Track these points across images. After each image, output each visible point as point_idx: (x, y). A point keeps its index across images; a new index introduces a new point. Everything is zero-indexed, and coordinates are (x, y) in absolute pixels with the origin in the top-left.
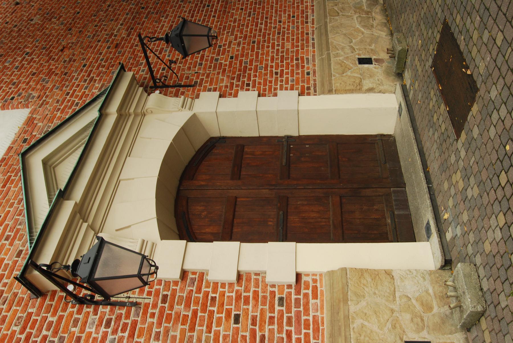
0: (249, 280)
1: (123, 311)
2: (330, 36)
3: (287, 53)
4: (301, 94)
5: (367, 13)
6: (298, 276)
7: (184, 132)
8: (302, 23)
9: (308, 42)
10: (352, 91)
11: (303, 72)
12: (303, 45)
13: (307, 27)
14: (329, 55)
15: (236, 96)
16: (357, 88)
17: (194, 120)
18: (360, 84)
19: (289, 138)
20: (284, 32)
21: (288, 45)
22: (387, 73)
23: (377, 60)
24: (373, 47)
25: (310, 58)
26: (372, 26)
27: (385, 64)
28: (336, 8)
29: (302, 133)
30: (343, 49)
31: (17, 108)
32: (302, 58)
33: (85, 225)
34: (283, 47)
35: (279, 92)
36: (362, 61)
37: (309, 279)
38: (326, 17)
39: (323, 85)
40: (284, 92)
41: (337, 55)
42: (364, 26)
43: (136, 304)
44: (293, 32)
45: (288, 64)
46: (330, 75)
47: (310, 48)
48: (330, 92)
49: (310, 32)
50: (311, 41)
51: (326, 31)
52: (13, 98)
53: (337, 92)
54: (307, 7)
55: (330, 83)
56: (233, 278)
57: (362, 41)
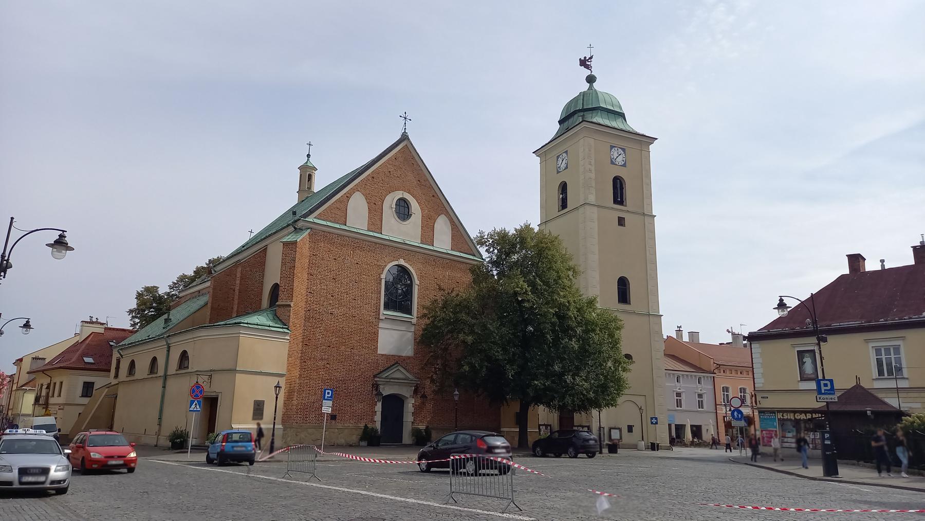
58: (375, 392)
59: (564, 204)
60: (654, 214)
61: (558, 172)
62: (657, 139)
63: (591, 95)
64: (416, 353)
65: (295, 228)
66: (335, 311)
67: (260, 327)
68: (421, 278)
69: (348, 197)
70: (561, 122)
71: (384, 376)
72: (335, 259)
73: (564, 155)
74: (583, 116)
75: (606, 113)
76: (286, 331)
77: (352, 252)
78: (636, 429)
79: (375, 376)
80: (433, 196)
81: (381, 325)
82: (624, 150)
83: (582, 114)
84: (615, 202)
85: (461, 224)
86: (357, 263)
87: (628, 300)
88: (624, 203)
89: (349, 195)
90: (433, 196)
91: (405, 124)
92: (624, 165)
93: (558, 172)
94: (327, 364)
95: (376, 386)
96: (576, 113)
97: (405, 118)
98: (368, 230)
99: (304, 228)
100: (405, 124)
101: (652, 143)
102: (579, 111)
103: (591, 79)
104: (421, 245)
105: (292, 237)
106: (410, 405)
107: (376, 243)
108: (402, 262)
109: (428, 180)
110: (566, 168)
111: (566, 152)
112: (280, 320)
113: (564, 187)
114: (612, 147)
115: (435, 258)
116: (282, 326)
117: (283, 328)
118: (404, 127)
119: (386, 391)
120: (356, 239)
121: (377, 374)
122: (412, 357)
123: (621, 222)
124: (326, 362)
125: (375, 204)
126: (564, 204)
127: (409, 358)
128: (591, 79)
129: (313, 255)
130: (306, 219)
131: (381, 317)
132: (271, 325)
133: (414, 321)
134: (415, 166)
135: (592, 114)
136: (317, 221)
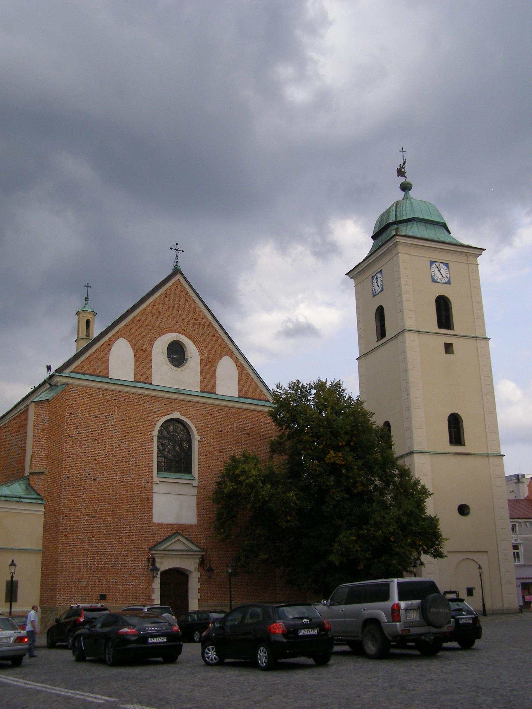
1: (147, 567)
6: (154, 600)
7: (188, 570)
15: (199, 582)
17: (191, 572)
21: (219, 595)
33: (163, 556)
40: (200, 594)
43: (148, 569)
52: (200, 516)
56: (153, 587)
58: (150, 567)
59: (382, 333)
60: (488, 336)
61: (374, 296)
62: (484, 250)
63: (405, 204)
64: (198, 522)
65: (51, 385)
66: (99, 476)
67: (8, 499)
68: (201, 432)
69: (110, 344)
70: (374, 237)
71: (162, 548)
72: (97, 417)
73: (379, 275)
74: (397, 230)
75: (423, 224)
76: (39, 501)
77: (116, 408)
78: (477, 592)
79: (150, 549)
80: (214, 336)
81: (156, 488)
82: (447, 265)
83: (395, 227)
84: (440, 326)
85: (250, 365)
86: (123, 420)
87: (463, 443)
88: (452, 326)
89: (111, 343)
90: (214, 336)
91: (177, 256)
92: (449, 283)
93: (374, 296)
94: (93, 537)
95: (152, 561)
97: (177, 250)
98: (136, 381)
99: (59, 384)
100: (177, 256)
101: (481, 255)
102: (393, 223)
103: (405, 187)
104: (201, 394)
105: (46, 395)
106: (196, 580)
107: (145, 396)
108: (176, 415)
109: (205, 318)
110: (382, 290)
111: (381, 272)
112: (34, 490)
113: (380, 312)
114: (432, 262)
115: (219, 408)
116: (34, 497)
117: (36, 499)
118: (176, 260)
119: (164, 565)
120: (121, 392)
121: (153, 547)
122: (195, 525)
123: (448, 348)
125: (142, 350)
126: (382, 333)
127: (191, 526)
128: (405, 187)
129: (71, 414)
130: (62, 375)
131: (156, 479)
132: (22, 496)
133: (196, 483)
134: (190, 303)
135: (407, 226)
136: (72, 375)
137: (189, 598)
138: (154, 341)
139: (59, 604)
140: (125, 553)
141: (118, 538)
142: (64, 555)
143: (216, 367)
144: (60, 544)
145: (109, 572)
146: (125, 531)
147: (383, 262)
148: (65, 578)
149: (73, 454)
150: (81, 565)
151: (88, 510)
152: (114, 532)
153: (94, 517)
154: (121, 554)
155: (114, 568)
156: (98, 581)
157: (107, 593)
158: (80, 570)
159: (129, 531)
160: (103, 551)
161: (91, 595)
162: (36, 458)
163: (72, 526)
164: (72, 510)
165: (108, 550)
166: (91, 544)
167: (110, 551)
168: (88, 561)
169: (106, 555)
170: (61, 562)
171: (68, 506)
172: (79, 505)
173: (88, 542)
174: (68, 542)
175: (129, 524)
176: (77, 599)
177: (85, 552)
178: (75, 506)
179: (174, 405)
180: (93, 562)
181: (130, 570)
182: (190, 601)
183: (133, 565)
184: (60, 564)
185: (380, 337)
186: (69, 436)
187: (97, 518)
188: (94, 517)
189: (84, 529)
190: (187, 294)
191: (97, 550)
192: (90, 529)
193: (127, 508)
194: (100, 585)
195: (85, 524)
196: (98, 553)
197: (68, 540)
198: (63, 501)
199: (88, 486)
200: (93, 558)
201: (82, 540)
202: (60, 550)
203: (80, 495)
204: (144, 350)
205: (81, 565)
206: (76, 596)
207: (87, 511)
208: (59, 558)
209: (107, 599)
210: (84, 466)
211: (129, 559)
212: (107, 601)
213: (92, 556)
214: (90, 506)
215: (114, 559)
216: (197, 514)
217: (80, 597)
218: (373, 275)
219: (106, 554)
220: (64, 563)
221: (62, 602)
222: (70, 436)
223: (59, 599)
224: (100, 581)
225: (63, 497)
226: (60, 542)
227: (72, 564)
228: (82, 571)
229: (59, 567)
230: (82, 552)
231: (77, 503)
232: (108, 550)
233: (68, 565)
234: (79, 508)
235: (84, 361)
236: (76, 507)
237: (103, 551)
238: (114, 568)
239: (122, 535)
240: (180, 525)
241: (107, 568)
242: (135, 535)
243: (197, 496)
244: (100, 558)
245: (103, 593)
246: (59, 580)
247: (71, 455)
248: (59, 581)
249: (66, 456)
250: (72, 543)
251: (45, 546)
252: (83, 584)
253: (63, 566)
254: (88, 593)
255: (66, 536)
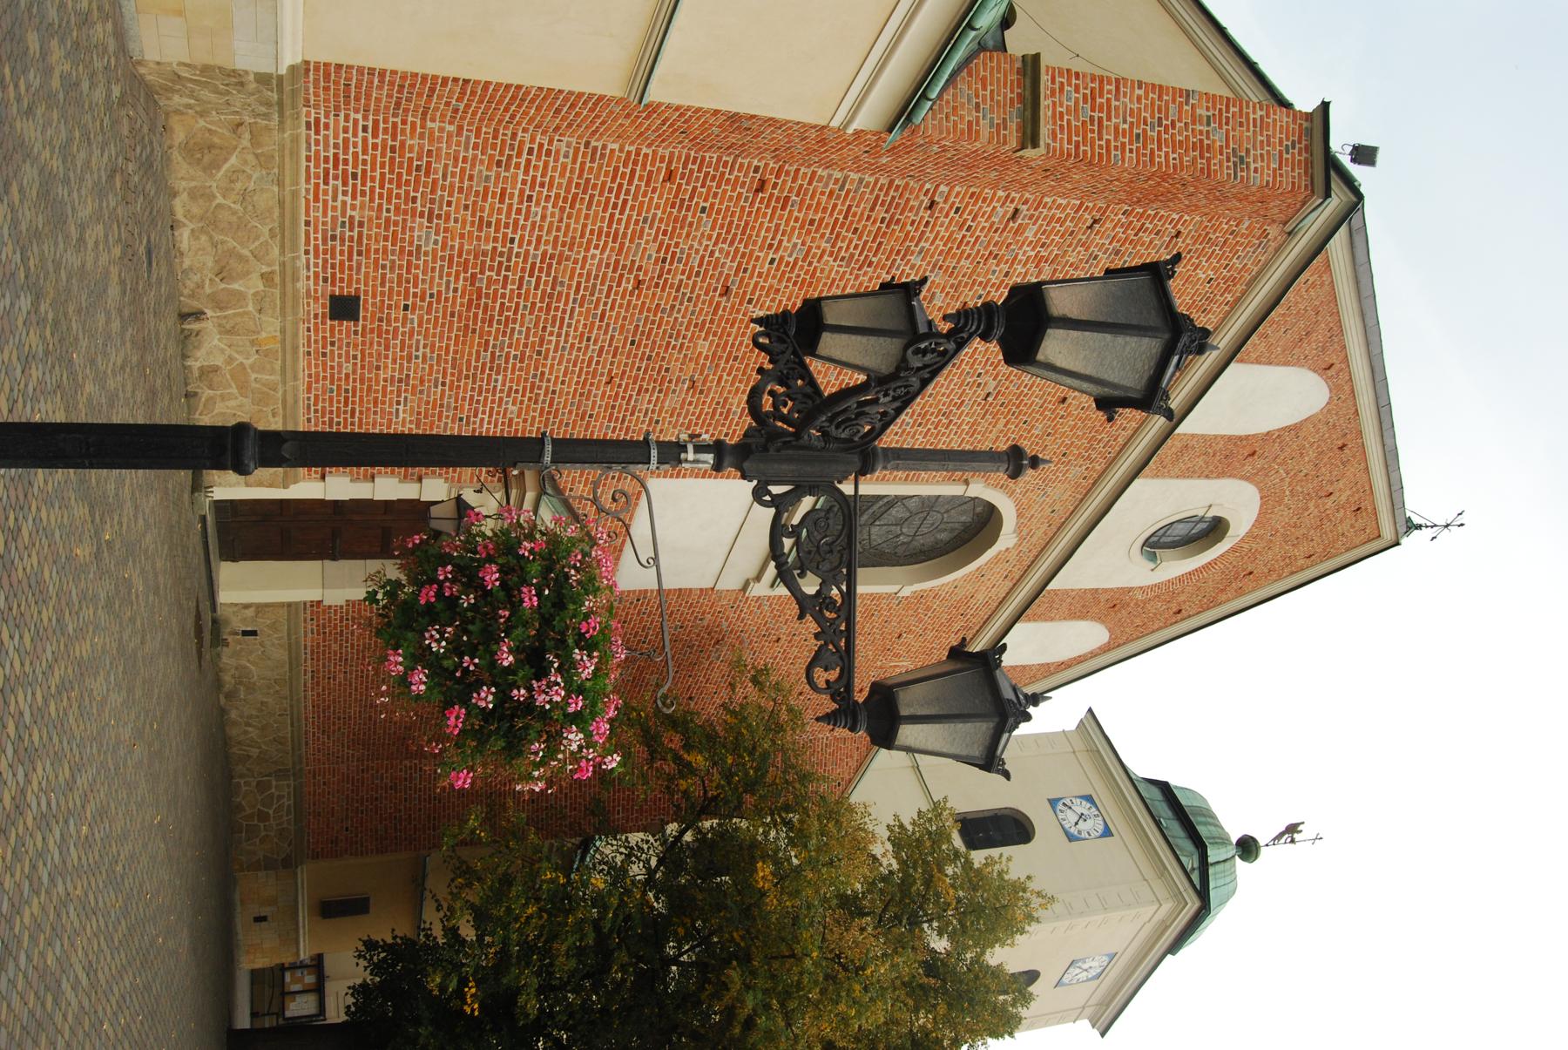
0: (365, 476)
2: (287, 659)
3: (336, 639)
4: (319, 602)
5: (241, 683)
8: (318, 671)
9: (312, 653)
10: (267, 605)
11: (318, 621)
12: (318, 647)
13: (312, 666)
14: (289, 639)
16: (261, 608)
18: (257, 613)
19: (334, 558)
20: (341, 660)
22: (227, 622)
23: (237, 634)
24: (238, 647)
25: (310, 635)
26: (237, 668)
27: (228, 630)
28: (278, 688)
29: (319, 563)
30: (273, 645)
31: (629, 592)
32: (318, 634)
34: (341, 645)
35: (344, 604)
36: (254, 633)
37: (314, 475)
38: (290, 678)
39: (297, 609)
41: (280, 639)
42: (246, 667)
44: (330, 661)
45: (335, 628)
46: (289, 620)
47: (309, 644)
48: (289, 605)
49: (309, 662)
50: (308, 651)
51: (290, 663)
53: (282, 605)
54: (313, 689)
55: (289, 612)
57: (251, 652)
61: (1053, 803)
69: (1332, 368)
70: (1164, 787)
80: (1179, 612)
90: (1179, 612)
93: (1053, 803)
94: (639, 283)
96: (1197, 847)
107: (1111, 462)
108: (1007, 539)
109: (1240, 592)
111: (1107, 833)
124: (652, 269)
137: (327, 563)
138: (1256, 485)
139: (317, 121)
140: (542, 392)
141: (610, 371)
142: (574, 162)
143: (1093, 619)
144: (632, 148)
145: (465, 336)
146: (638, 394)
147: (1129, 838)
148: (456, 159)
149: (1019, 231)
150: (515, 232)
151: (765, 270)
152: (642, 359)
153: (726, 291)
154: (541, 381)
155: (478, 352)
156: (424, 293)
157: (361, 322)
158: (489, 224)
159: (635, 407)
160: (567, 316)
161: (359, 265)
162: (1093, 99)
163: (707, 205)
164: (783, 208)
165: (567, 335)
166: (605, 274)
167: (558, 342)
168: (525, 261)
169: (544, 328)
170: (541, 145)
171: (805, 194)
172: (794, 240)
173: (617, 262)
174: (636, 182)
175: (662, 407)
176: (339, 204)
177: (571, 250)
178: (798, 225)
179: (1039, 533)
180: (522, 278)
181: (462, 406)
182: (315, 566)
183: (486, 417)
184: (532, 140)
185: (960, 817)
186: (1095, 221)
187: (718, 304)
188: (726, 291)
189: (682, 252)
190: (1329, 556)
191: (572, 296)
192: (675, 275)
193: (732, 404)
194: (406, 298)
195: (703, 257)
196: (558, 301)
197: (647, 184)
198: (838, 175)
199: (866, 278)
200: (539, 278)
201: (631, 241)
202: (604, 147)
203: (839, 244)
204: (1250, 459)
205: (515, 232)
206: (354, 197)
207: (762, 267)
208: (565, 139)
209: (336, 323)
210: (954, 268)
211: (510, 406)
212: (324, 323)
213: (548, 275)
214: (780, 281)
215: (523, 354)
216: (646, 591)
217: (352, 217)
218: (1097, 801)
219: (549, 329)
220: (533, 158)
221: (326, 137)
222: (1097, 226)
223: (342, 124)
224: (423, 300)
225: (853, 176)
226: (645, 150)
227: (522, 191)
228: (480, 229)
229: (514, 135)
230: (574, 238)
231: (809, 232)
232: (567, 335)
233: (521, 177)
234: (786, 238)
235: (1333, 297)
236: (794, 229)
237: (567, 316)
238: (478, 352)
239: (620, 386)
240: (621, 551)
241: (482, 328)
242: (612, 425)
243: (713, 589)
244: (534, 304)
245: (366, 310)
246: (452, 128)
247: (1019, 221)
248: (441, 130)
249: (1025, 203)
250: (625, 201)
251: (653, 109)
252: (416, 234)
253: (519, 155)
254: (368, 251)
255: (670, 176)
